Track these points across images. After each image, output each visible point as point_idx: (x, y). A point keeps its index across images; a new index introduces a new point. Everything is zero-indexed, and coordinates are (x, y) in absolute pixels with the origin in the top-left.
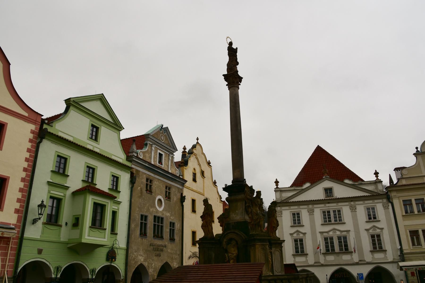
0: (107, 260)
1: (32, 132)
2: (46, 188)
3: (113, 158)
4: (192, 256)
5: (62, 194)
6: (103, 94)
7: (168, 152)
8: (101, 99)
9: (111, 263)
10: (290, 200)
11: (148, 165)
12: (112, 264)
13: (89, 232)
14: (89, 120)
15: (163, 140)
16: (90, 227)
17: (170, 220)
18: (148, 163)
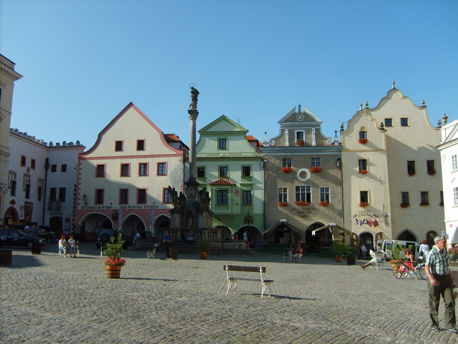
0: (245, 222)
1: (180, 161)
3: (244, 155)
4: (358, 214)
6: (223, 115)
7: (310, 126)
8: (223, 118)
9: (249, 224)
10: (451, 139)
11: (278, 148)
12: (249, 225)
13: (215, 207)
14: (216, 137)
15: (301, 119)
16: (216, 205)
17: (322, 187)
18: (278, 148)
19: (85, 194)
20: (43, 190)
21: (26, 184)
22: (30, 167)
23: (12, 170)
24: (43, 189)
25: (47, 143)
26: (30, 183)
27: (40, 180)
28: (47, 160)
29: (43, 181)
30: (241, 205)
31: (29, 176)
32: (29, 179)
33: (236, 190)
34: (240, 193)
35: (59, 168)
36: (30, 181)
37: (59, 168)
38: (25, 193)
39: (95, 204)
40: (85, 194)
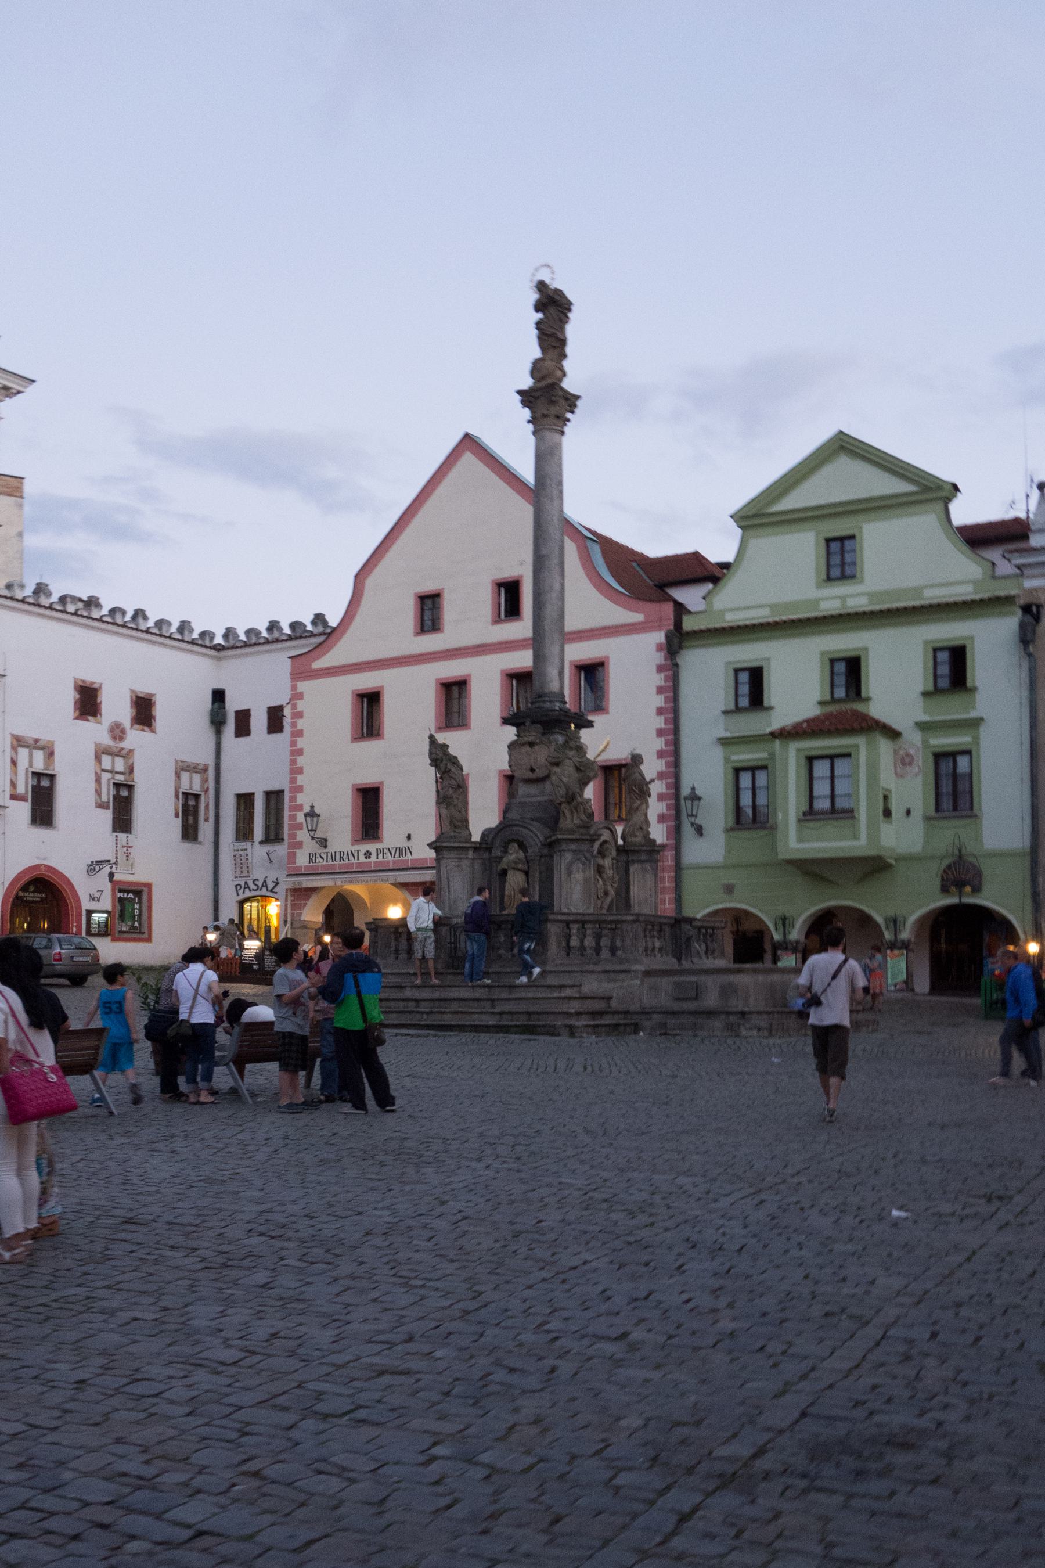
2: (719, 752)
5: (765, 755)
19: (312, 807)
20: (207, 806)
21: (109, 785)
22: (126, 721)
23: (29, 733)
24: (207, 802)
25: (169, 624)
26: (133, 781)
27: (182, 768)
28: (219, 696)
29: (205, 769)
30: (928, 819)
31: (127, 755)
32: (126, 763)
33: (902, 752)
34: (923, 764)
35: (259, 721)
36: (131, 770)
37: (259, 721)
38: (107, 816)
39: (355, 842)
40: (312, 807)
